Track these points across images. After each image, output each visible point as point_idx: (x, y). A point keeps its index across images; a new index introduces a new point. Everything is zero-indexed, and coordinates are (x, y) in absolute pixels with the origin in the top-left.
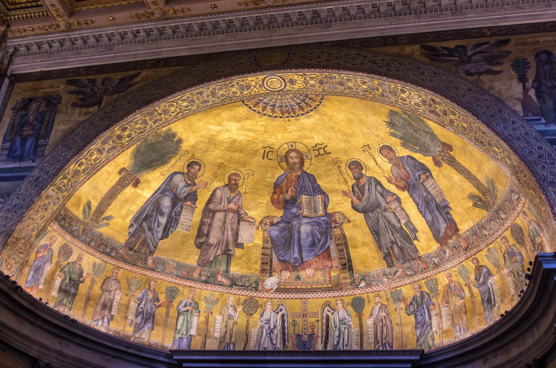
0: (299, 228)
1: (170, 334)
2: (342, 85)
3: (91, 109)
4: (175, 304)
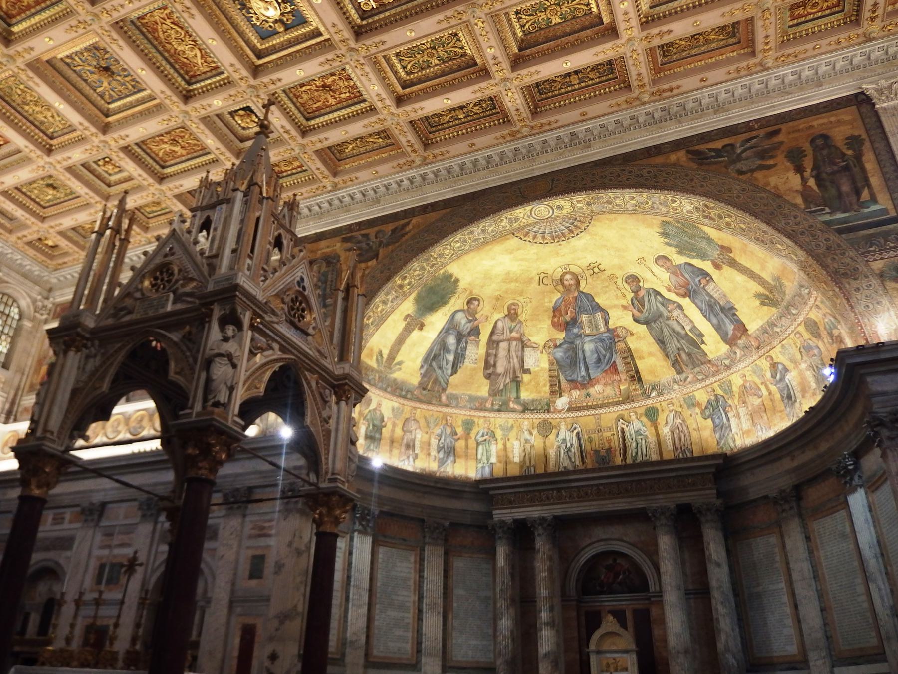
0: (583, 347)
2: (610, 204)
3: (370, 263)
4: (473, 435)
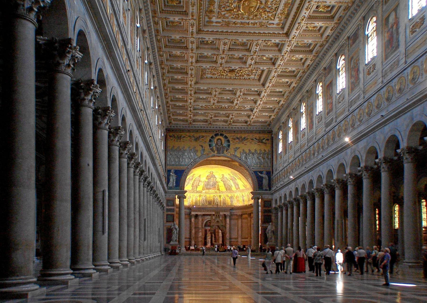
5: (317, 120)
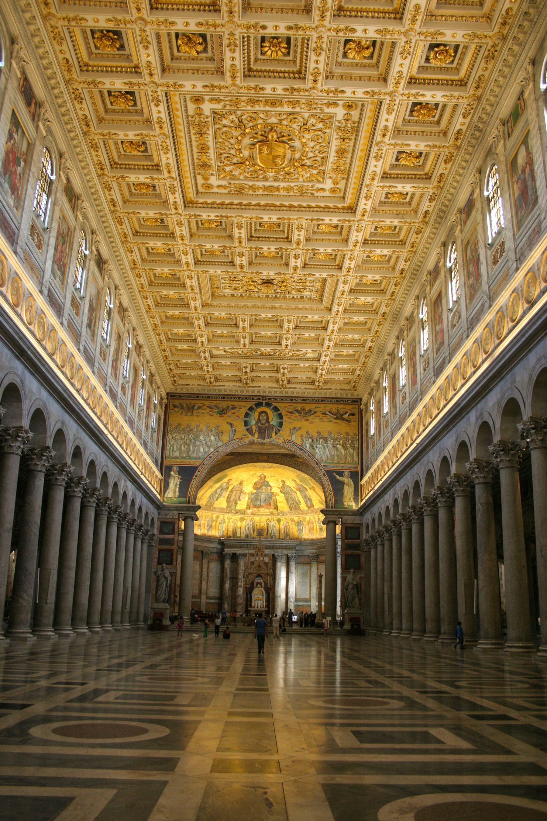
1: (217, 531)
5: (422, 366)
